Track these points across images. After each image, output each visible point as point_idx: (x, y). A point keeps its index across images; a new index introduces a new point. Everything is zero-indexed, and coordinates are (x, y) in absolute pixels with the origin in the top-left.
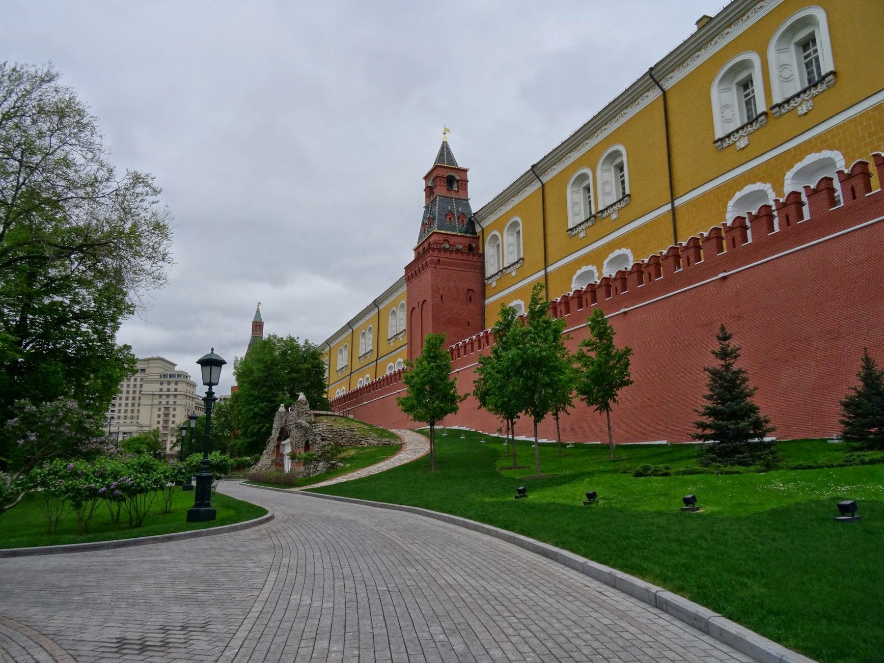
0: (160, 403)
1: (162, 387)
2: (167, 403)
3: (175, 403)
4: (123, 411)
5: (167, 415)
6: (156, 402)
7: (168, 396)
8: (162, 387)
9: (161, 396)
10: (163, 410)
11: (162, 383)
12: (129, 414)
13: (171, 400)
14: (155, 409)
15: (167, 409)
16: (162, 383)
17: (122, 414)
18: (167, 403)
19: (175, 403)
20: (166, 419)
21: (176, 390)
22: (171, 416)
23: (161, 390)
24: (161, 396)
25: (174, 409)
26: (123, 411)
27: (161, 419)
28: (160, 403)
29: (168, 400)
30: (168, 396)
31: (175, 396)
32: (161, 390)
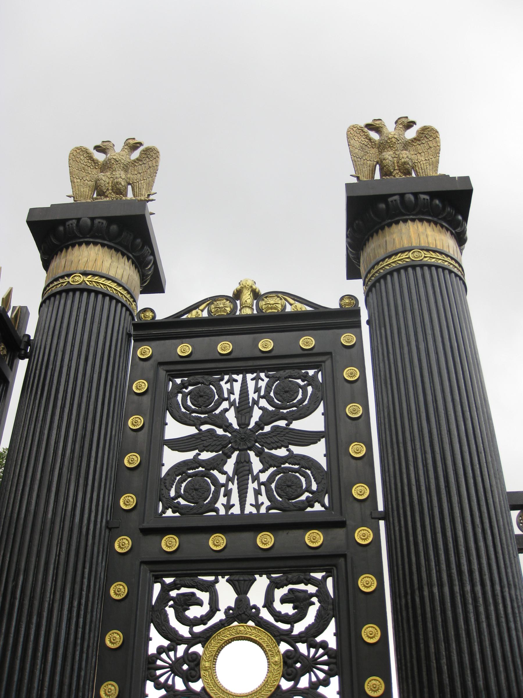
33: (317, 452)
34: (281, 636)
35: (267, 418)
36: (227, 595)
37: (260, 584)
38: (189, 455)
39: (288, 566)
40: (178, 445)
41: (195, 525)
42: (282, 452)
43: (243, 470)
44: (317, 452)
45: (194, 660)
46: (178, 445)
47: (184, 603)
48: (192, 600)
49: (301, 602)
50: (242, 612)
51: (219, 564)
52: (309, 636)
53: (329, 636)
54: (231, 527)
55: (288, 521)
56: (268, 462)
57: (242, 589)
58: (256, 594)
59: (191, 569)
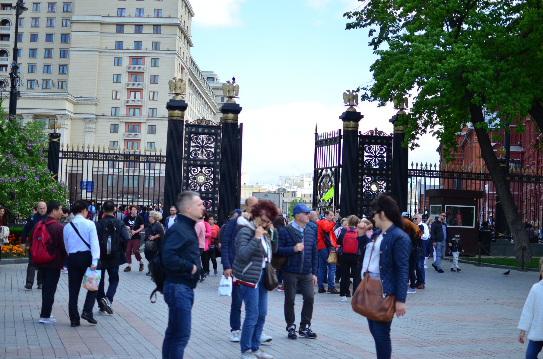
0: (119, 45)
2: (138, 45)
3: (156, 45)
6: (110, 41)
7: (139, 27)
9: (120, 27)
10: (126, 62)
13: (147, 39)
14: (110, 59)
15: (135, 60)
18: (138, 45)
19: (156, 45)
21: (158, 12)
22: (147, 78)
24: (120, 27)
25: (155, 63)
27: (122, 86)
28: (119, 45)
29: (138, 37)
30: (139, 27)
31: (157, 27)
33: (213, 150)
34: (206, 175)
35: (206, 144)
36: (199, 170)
37: (204, 169)
38: (194, 149)
39: (208, 166)
40: (193, 147)
41: (195, 160)
42: (208, 149)
43: (202, 152)
44: (213, 150)
45: (195, 178)
46: (193, 147)
47: (194, 170)
48: (195, 170)
49: (209, 171)
50: (201, 172)
51: (198, 166)
52: (209, 176)
53: (212, 176)
54: (200, 160)
55: (208, 161)
56: (206, 151)
57: (201, 169)
58: (203, 170)
59: (195, 166)
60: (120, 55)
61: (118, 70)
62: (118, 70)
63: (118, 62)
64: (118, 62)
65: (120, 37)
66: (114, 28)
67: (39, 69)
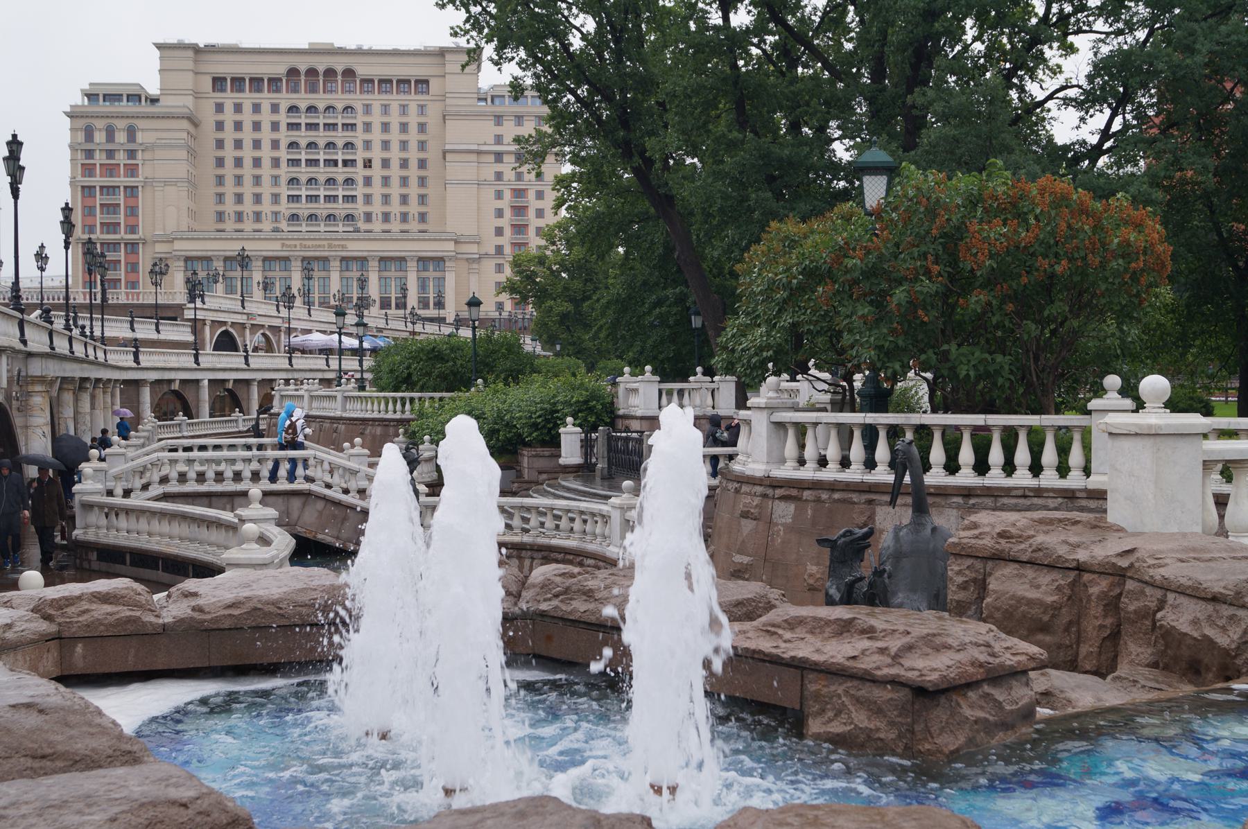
0: (499, 176)
1: (499, 130)
4: (377, 199)
5: (519, 210)
8: (499, 130)
9: (499, 157)
10: (507, 195)
11: (499, 119)
12: (395, 208)
14: (489, 193)
16: (499, 119)
17: (377, 208)
20: (519, 221)
23: (499, 139)
24: (499, 157)
26: (377, 199)
27: (505, 222)
28: (499, 176)
32: (499, 139)
60: (500, 188)
61: (499, 204)
62: (499, 204)
63: (499, 195)
64: (499, 195)
65: (499, 167)
66: (492, 158)
67: (395, 200)
